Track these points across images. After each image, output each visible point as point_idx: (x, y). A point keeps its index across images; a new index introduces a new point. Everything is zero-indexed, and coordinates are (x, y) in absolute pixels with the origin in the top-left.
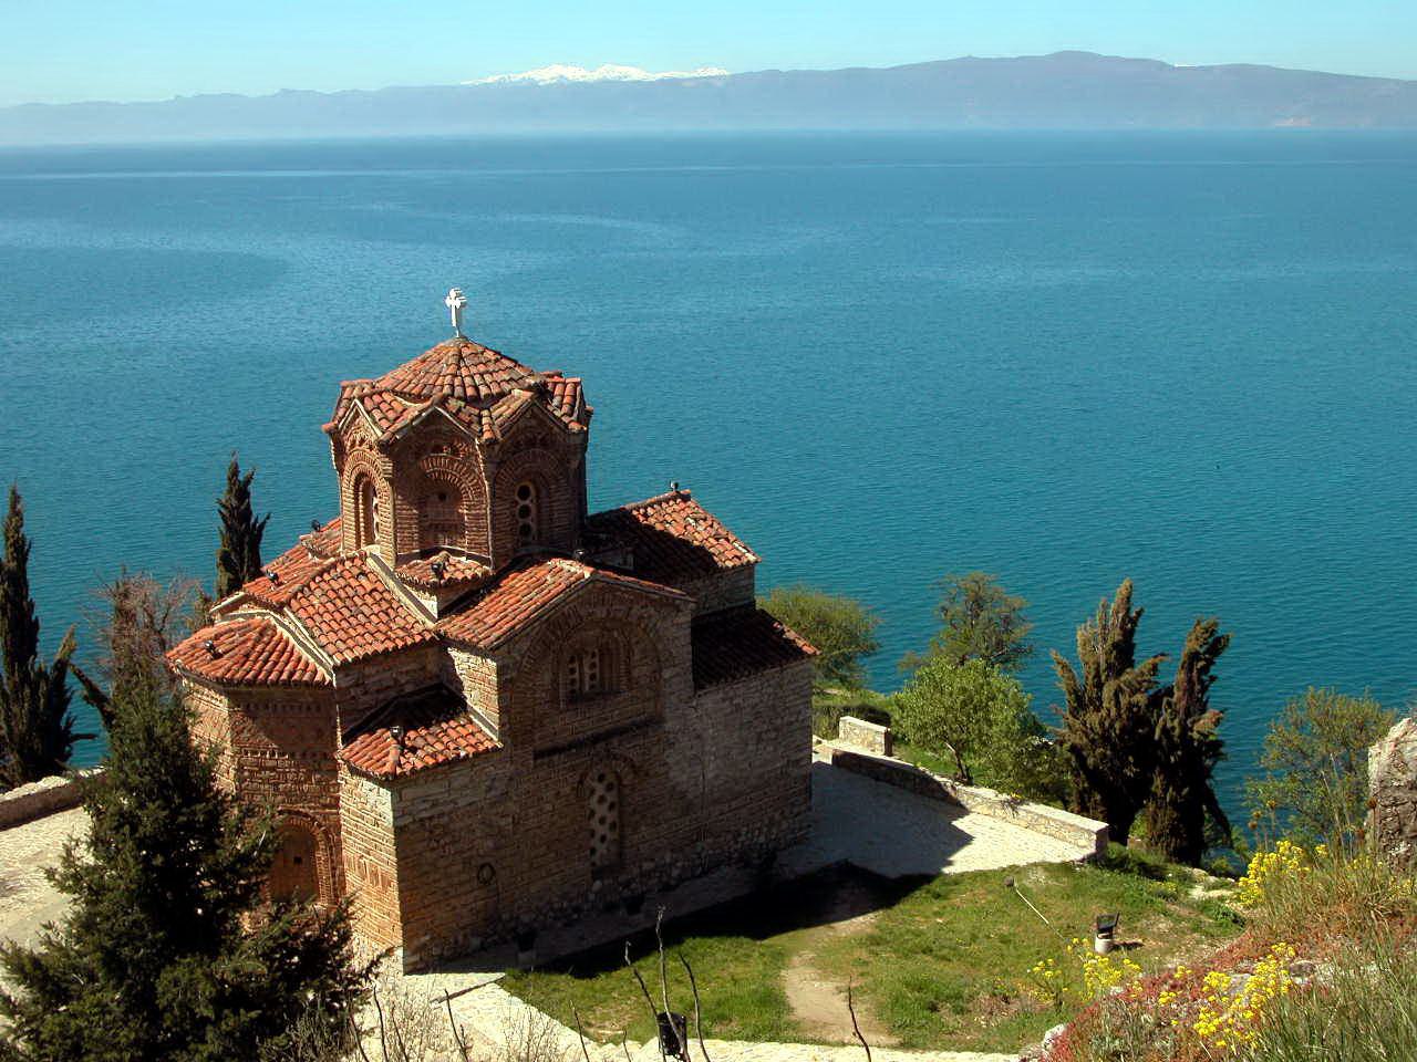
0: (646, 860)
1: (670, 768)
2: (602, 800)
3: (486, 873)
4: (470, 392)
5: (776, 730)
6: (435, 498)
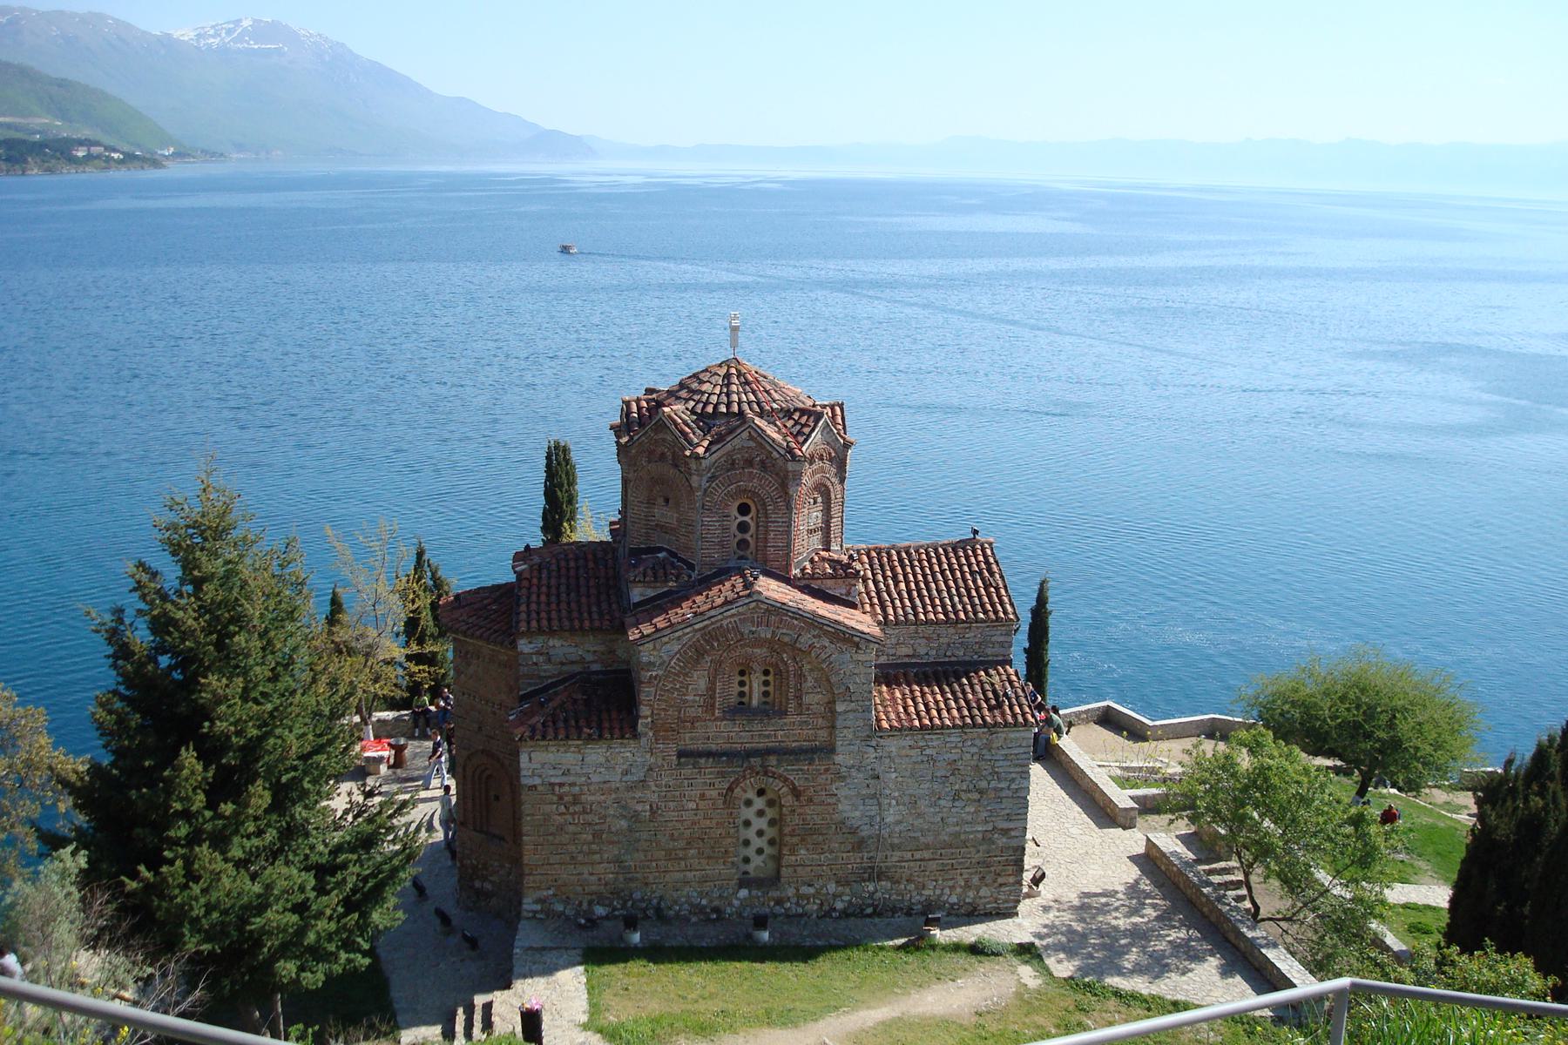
0: (804, 883)
2: (761, 813)
4: (710, 409)
5: (981, 792)
6: (661, 501)
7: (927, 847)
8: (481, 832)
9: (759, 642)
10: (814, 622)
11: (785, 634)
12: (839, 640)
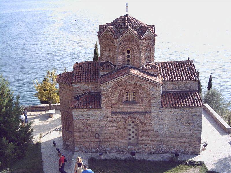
1: (153, 125)
2: (133, 128)
3: (97, 136)
4: (120, 27)
7: (175, 137)
8: (67, 131)
9: (131, 85)
10: (145, 80)
11: (138, 83)
12: (152, 84)
